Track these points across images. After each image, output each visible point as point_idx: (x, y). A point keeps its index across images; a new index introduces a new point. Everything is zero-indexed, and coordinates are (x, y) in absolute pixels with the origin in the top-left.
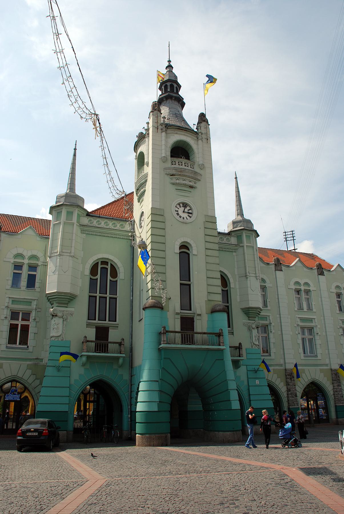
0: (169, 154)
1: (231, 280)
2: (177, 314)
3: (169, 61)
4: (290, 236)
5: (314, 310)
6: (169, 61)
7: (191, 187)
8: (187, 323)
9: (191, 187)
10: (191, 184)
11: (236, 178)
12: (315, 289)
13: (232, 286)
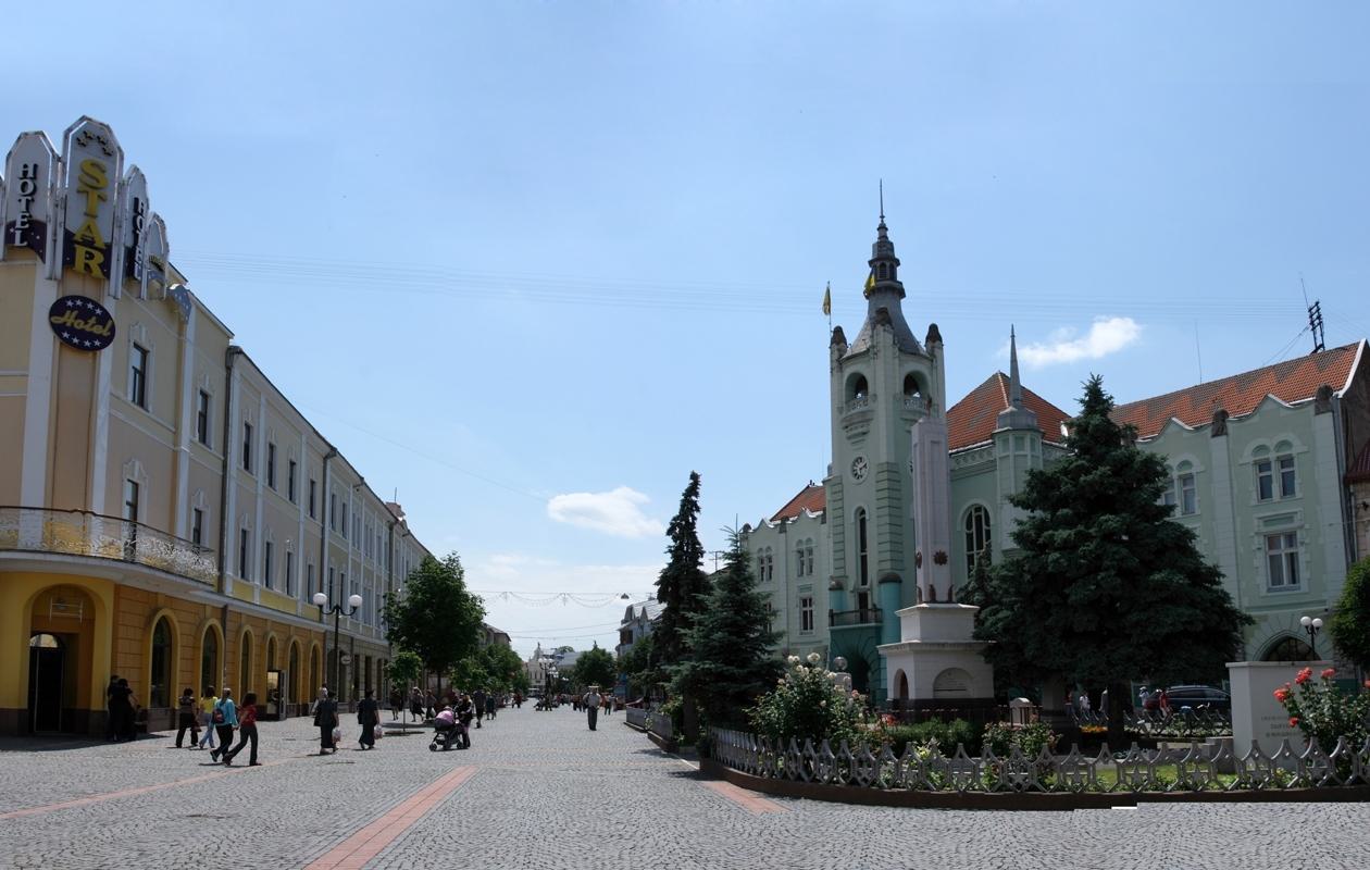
0: (844, 400)
1: (991, 514)
2: (852, 592)
3: (882, 217)
4: (1316, 319)
5: (1198, 512)
6: (882, 217)
7: (864, 433)
8: (863, 598)
9: (864, 433)
10: (860, 430)
11: (1013, 336)
12: (1202, 468)
13: (992, 523)
